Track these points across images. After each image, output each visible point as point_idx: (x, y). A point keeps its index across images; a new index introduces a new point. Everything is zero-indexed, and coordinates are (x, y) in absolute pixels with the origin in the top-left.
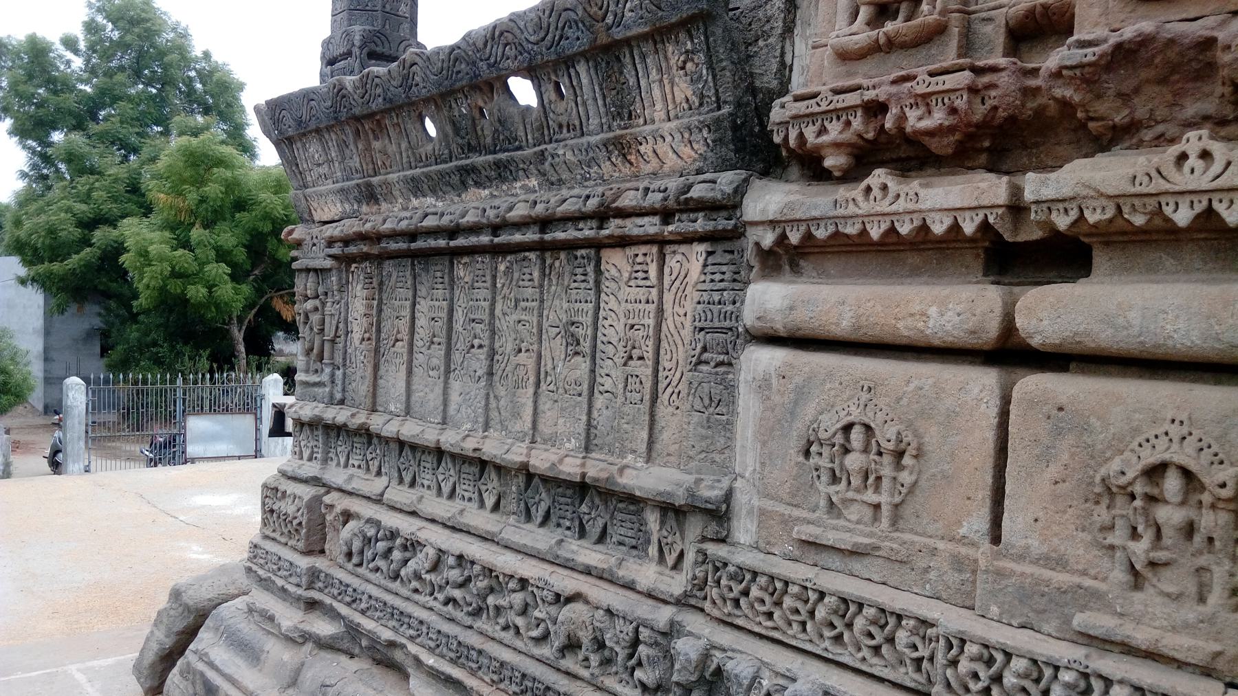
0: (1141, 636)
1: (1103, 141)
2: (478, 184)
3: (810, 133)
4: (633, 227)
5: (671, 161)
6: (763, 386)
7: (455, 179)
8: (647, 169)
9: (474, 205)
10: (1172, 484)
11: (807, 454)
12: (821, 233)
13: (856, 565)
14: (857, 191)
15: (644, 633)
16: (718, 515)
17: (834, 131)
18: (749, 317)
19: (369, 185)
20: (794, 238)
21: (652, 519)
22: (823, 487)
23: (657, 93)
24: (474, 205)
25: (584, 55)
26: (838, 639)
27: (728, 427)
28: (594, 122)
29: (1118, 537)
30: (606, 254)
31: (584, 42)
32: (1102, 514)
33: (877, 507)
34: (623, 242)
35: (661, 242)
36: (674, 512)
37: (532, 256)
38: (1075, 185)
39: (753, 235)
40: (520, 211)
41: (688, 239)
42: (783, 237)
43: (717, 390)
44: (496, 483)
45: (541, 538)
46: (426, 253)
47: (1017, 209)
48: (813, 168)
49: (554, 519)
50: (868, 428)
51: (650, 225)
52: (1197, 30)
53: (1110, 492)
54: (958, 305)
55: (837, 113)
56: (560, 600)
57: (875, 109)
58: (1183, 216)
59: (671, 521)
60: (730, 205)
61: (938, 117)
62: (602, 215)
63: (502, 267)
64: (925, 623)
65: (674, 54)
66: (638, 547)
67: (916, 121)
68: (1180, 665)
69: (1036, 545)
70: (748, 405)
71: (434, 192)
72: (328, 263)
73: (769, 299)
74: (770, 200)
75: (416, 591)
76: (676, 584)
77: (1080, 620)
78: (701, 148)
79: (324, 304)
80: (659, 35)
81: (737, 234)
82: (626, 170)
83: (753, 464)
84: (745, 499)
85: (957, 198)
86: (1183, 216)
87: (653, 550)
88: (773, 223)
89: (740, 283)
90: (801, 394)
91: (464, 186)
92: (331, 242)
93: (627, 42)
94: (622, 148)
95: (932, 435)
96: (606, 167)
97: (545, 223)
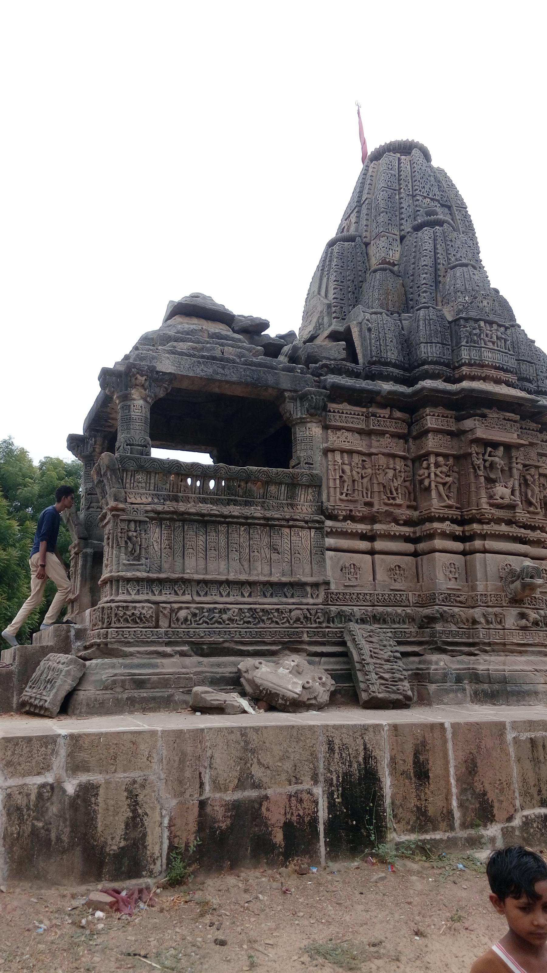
0: (398, 588)
1: (380, 522)
2: (234, 505)
3: (340, 512)
4: (297, 523)
5: (305, 511)
6: (331, 558)
7: (226, 502)
8: (298, 511)
9: (235, 510)
10: (397, 568)
11: (341, 570)
12: (339, 530)
13: (355, 588)
14: (346, 524)
15: (319, 611)
16: (327, 583)
17: (344, 513)
18: (327, 545)
19: (177, 496)
20: (334, 530)
21: (309, 589)
22: (347, 576)
23: (303, 496)
24: (235, 510)
25: (286, 484)
26: (357, 601)
27: (325, 567)
28: (282, 498)
29: (392, 576)
30: (283, 529)
31: (289, 481)
32: (389, 573)
33: (356, 578)
34: (290, 527)
35: (302, 527)
36: (316, 585)
37: (258, 527)
38: (377, 526)
39: (326, 529)
40: (258, 515)
41: (310, 528)
42: (332, 530)
43: (320, 560)
44: (249, 589)
45: (275, 600)
46: (205, 522)
47: (372, 530)
48: (332, 517)
49: (274, 595)
50: (354, 565)
51: (303, 524)
52: (392, 510)
53: (391, 570)
54: (364, 545)
55: (345, 510)
56: (291, 611)
57: (351, 511)
58: (392, 534)
59: (314, 588)
60: (323, 523)
61: (361, 514)
62: (288, 520)
63: (243, 529)
64: (371, 594)
65: (310, 490)
66: (305, 596)
67: (358, 514)
68: (402, 591)
69: (382, 579)
70: (328, 562)
71: (211, 504)
72: (148, 520)
73: (330, 541)
74: (329, 523)
75: (228, 624)
76: (320, 600)
77: (392, 588)
78: (313, 510)
79: (140, 534)
80: (308, 486)
81: (323, 528)
82: (292, 511)
83: (331, 573)
84: (332, 580)
85: (361, 527)
86: (392, 534)
87: (309, 595)
88: (330, 527)
89: (323, 537)
90: (339, 560)
91: (228, 504)
92: (147, 512)
93: (299, 485)
94: (292, 505)
95: (362, 565)
96: (286, 509)
97: (265, 518)
